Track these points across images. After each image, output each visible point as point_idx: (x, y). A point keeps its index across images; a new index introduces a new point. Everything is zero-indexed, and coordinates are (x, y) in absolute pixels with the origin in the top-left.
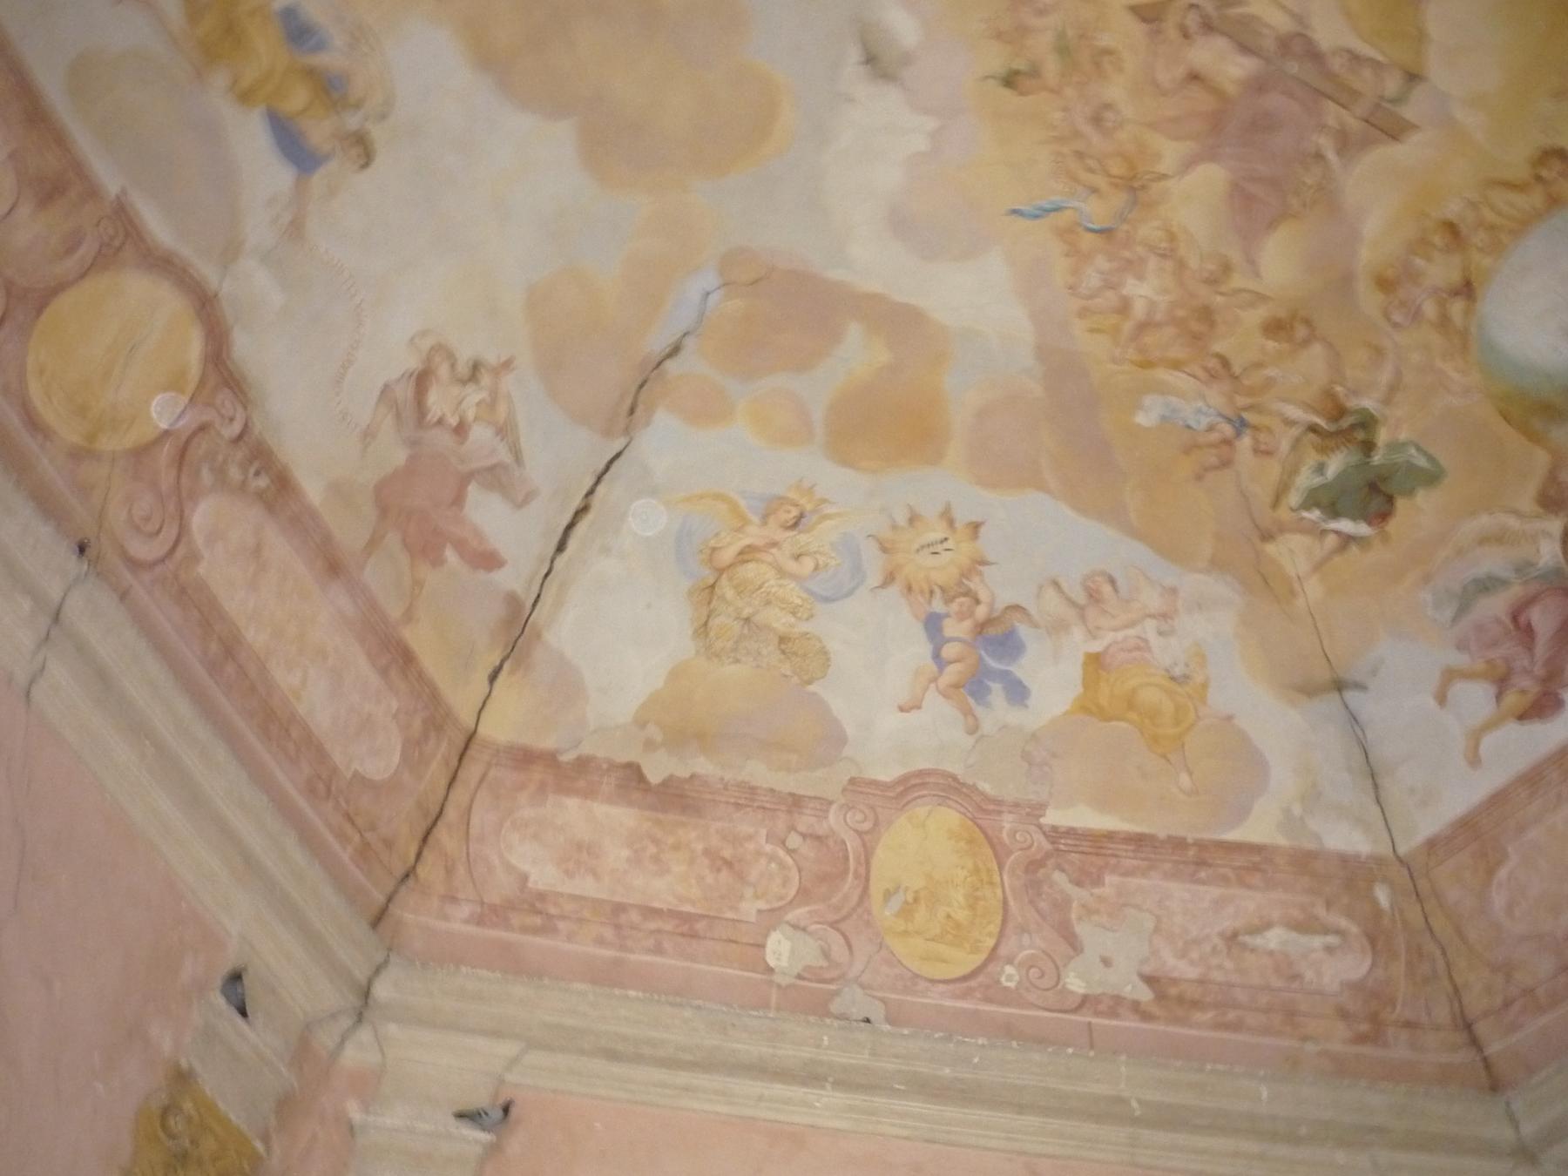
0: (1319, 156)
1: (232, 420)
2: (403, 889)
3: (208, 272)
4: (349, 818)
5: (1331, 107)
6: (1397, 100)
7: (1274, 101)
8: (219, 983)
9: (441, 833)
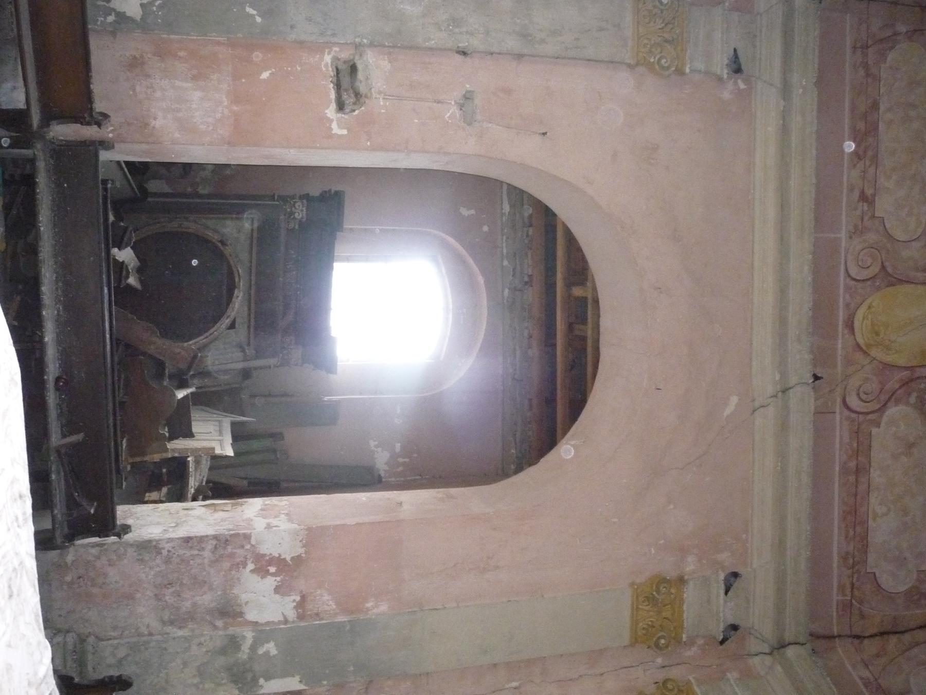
2: (850, 640)
4: (853, 585)
8: (728, 572)
9: (893, 639)
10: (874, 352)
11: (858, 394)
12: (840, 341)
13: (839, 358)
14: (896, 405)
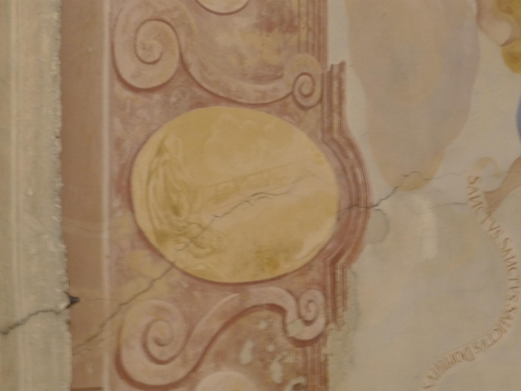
1: (308, 323)
3: (378, 186)
10: (170, 251)
11: (145, 346)
12: (106, 224)
13: (106, 263)
14: (217, 368)
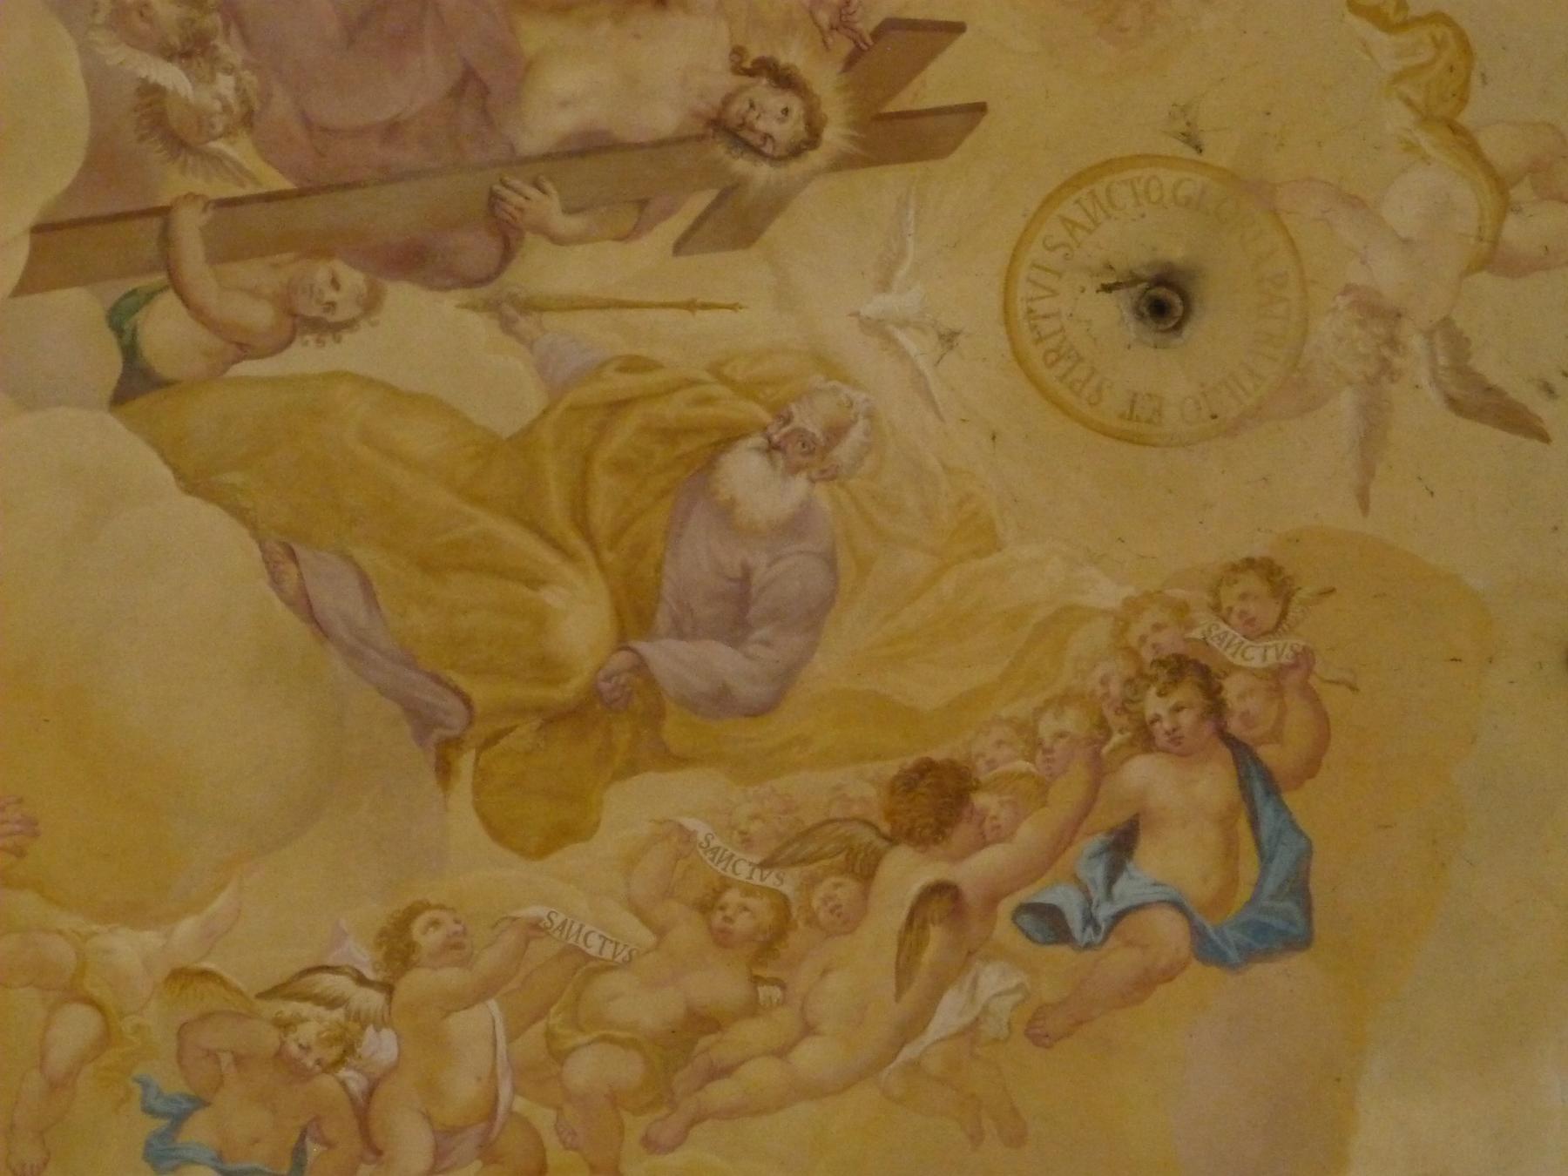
0: (192, 50)
5: (278, 182)
6: (121, 321)
7: (415, 86)
